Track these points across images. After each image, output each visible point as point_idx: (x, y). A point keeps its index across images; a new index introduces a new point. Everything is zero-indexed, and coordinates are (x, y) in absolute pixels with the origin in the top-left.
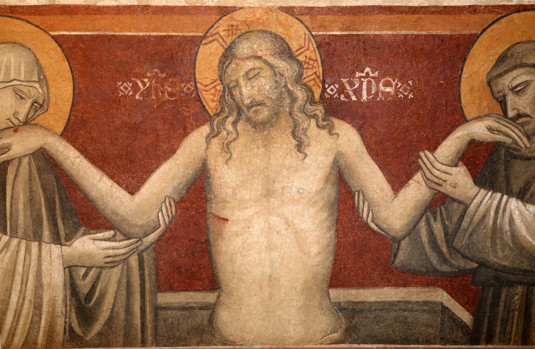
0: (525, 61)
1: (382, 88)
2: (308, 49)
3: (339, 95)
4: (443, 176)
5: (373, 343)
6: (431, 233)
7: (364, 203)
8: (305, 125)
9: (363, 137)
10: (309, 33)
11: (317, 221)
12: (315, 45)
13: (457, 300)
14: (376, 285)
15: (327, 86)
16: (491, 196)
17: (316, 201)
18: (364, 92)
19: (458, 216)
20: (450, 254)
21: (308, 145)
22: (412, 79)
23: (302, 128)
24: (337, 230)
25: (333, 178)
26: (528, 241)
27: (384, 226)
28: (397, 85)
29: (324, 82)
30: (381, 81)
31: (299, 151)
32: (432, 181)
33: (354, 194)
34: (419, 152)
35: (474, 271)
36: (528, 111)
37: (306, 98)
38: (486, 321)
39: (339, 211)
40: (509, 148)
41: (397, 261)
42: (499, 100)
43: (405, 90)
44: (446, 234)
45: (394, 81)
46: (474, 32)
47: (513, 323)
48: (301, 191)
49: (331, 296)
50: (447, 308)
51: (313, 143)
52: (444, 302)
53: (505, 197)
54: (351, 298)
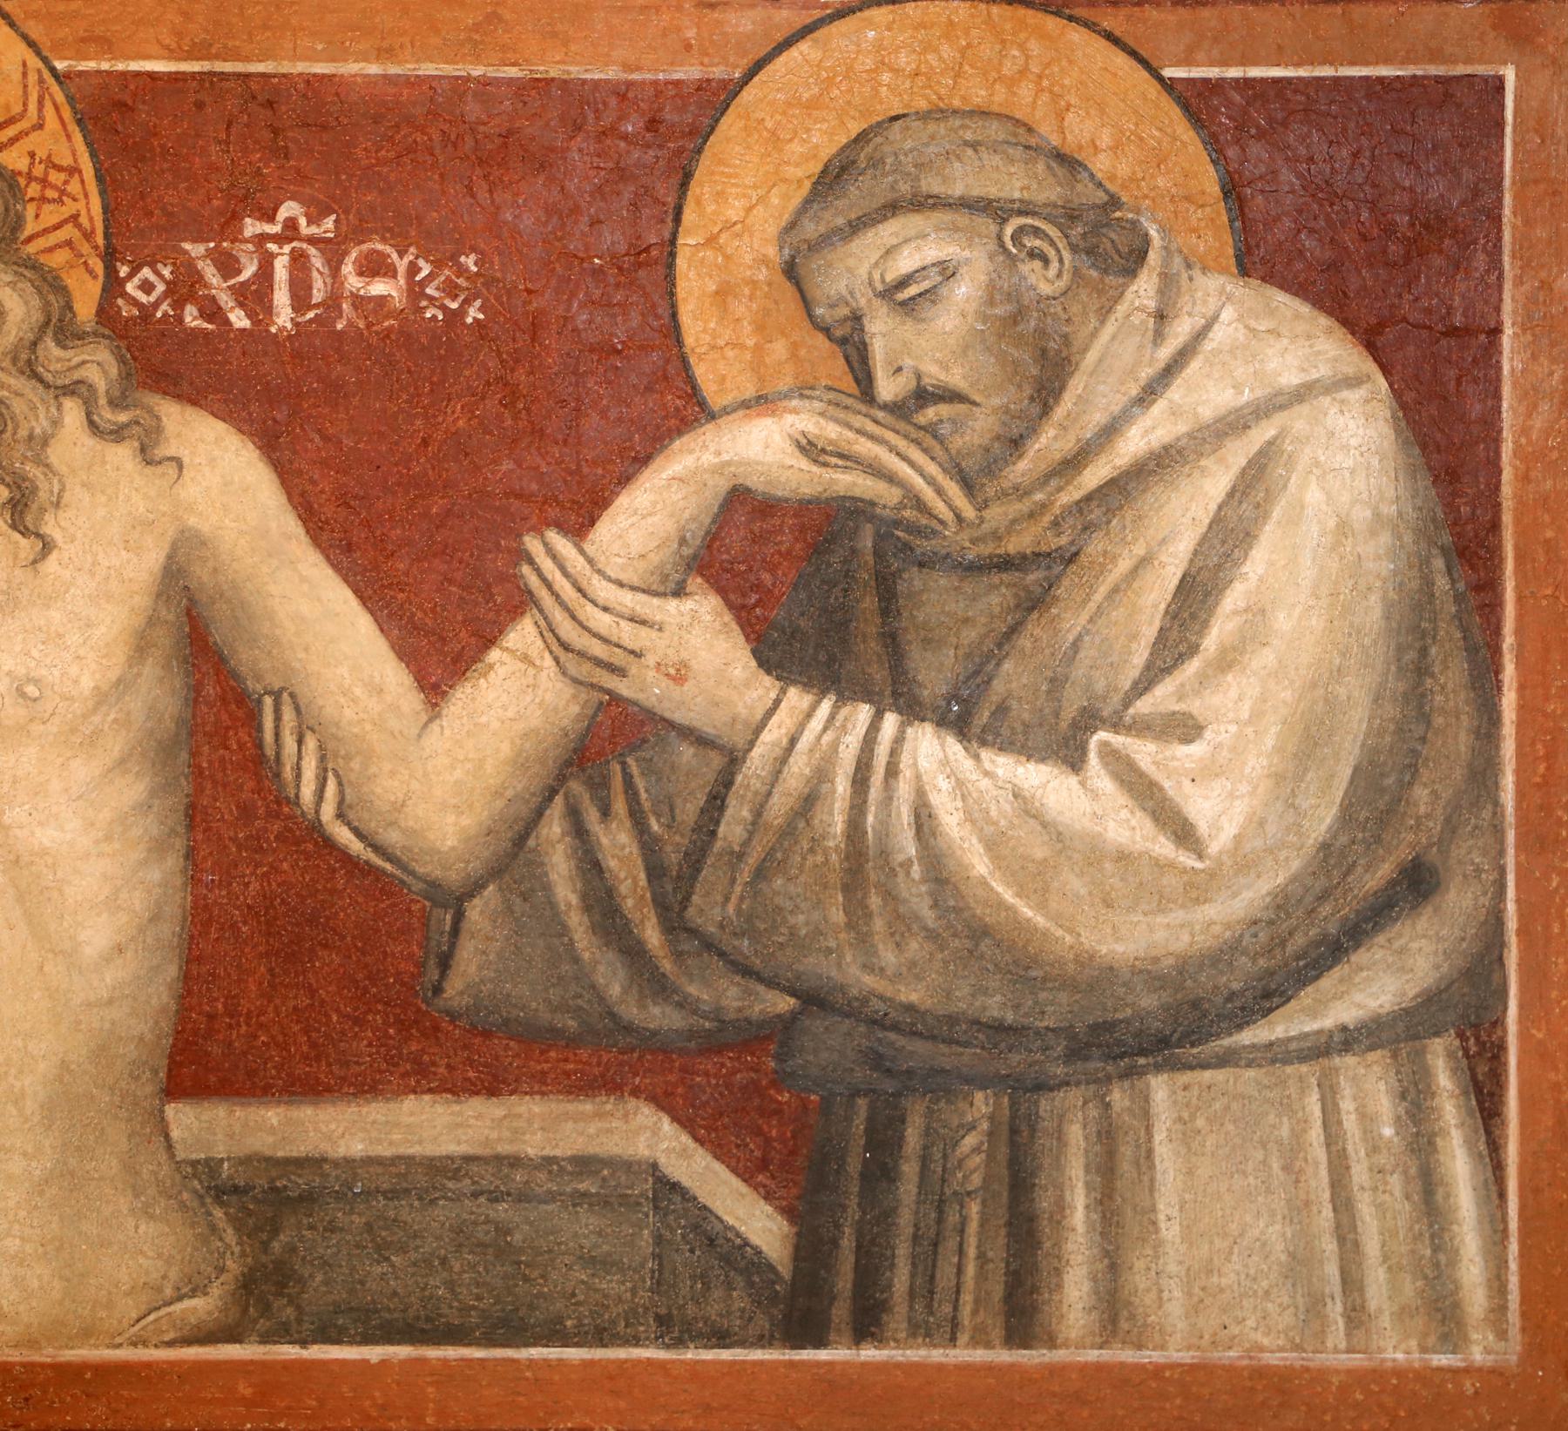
0: (931, 184)
1: (353, 282)
2: (40, 126)
3: (179, 305)
4: (627, 634)
5: (366, 1340)
6: (590, 865)
7: (300, 742)
8: (41, 425)
9: (286, 474)
10: (40, 65)
11: (106, 815)
12: (67, 113)
13: (720, 1152)
14: (367, 1087)
15: (124, 271)
16: (832, 717)
17: (97, 734)
18: (281, 298)
19: (701, 799)
20: (678, 956)
21: (57, 505)
22: (473, 249)
23: (23, 433)
24: (190, 854)
25: (164, 639)
26: (1001, 904)
27: (392, 838)
28: (413, 269)
29: (110, 256)
30: (346, 253)
31: (19, 526)
32: (581, 654)
33: (260, 702)
34: (520, 535)
35: (783, 1030)
36: (956, 378)
37: (37, 317)
38: (847, 1242)
39: (197, 772)
40: (897, 523)
41: (454, 987)
42: (839, 333)
43: (451, 290)
44: (655, 871)
45: (401, 255)
46: (718, 72)
47: (961, 1252)
48: (31, 690)
49: (175, 1134)
50: (675, 1187)
51: (76, 494)
52: (662, 1161)
53: (890, 721)
54: (262, 1143)
